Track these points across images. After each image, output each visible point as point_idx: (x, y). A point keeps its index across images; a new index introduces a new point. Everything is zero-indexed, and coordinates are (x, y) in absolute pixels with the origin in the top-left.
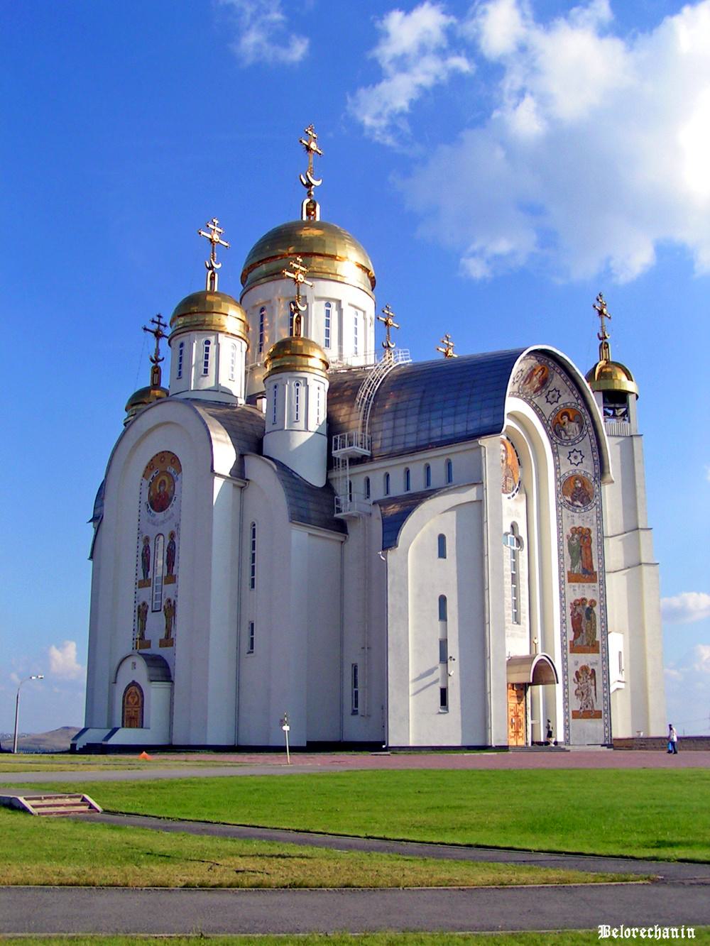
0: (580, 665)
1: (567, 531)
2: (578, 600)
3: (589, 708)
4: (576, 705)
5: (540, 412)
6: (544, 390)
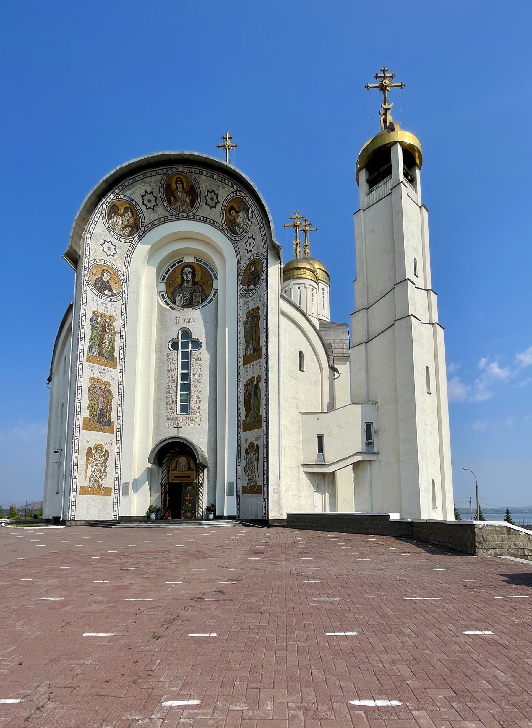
0: (249, 442)
1: (244, 319)
2: (249, 380)
3: (253, 484)
4: (245, 481)
5: (212, 222)
6: (199, 198)
